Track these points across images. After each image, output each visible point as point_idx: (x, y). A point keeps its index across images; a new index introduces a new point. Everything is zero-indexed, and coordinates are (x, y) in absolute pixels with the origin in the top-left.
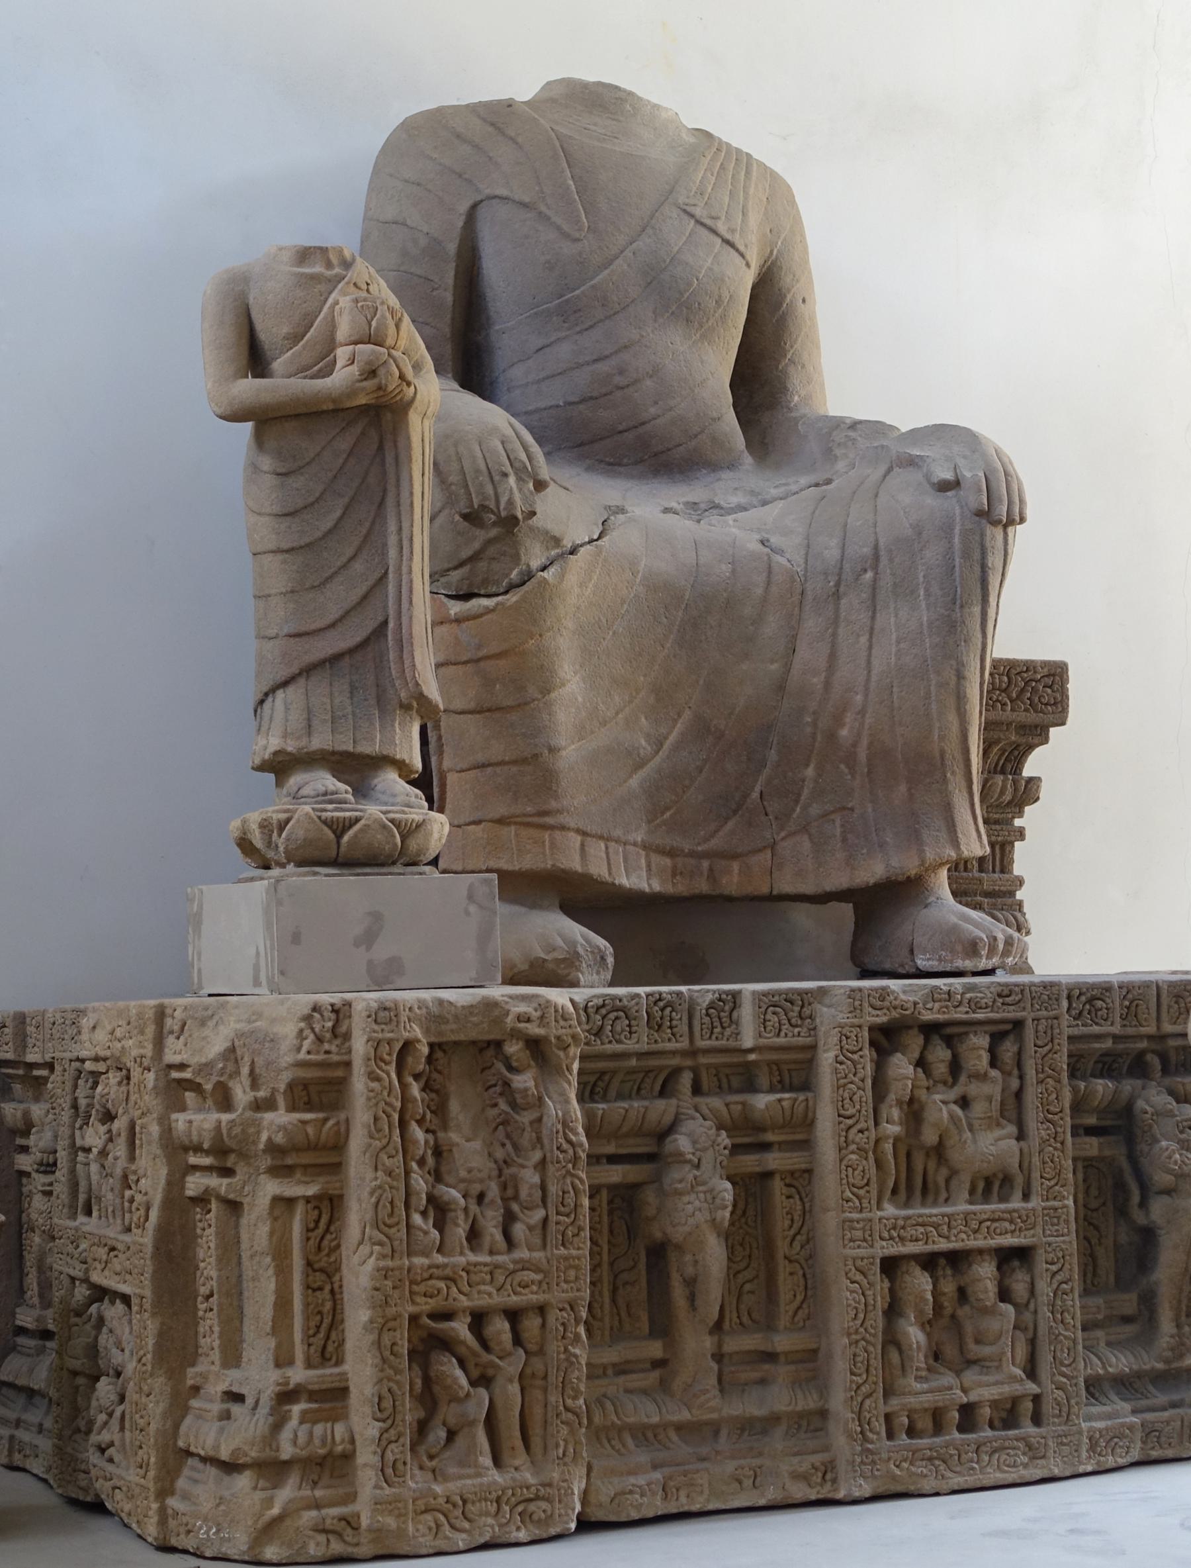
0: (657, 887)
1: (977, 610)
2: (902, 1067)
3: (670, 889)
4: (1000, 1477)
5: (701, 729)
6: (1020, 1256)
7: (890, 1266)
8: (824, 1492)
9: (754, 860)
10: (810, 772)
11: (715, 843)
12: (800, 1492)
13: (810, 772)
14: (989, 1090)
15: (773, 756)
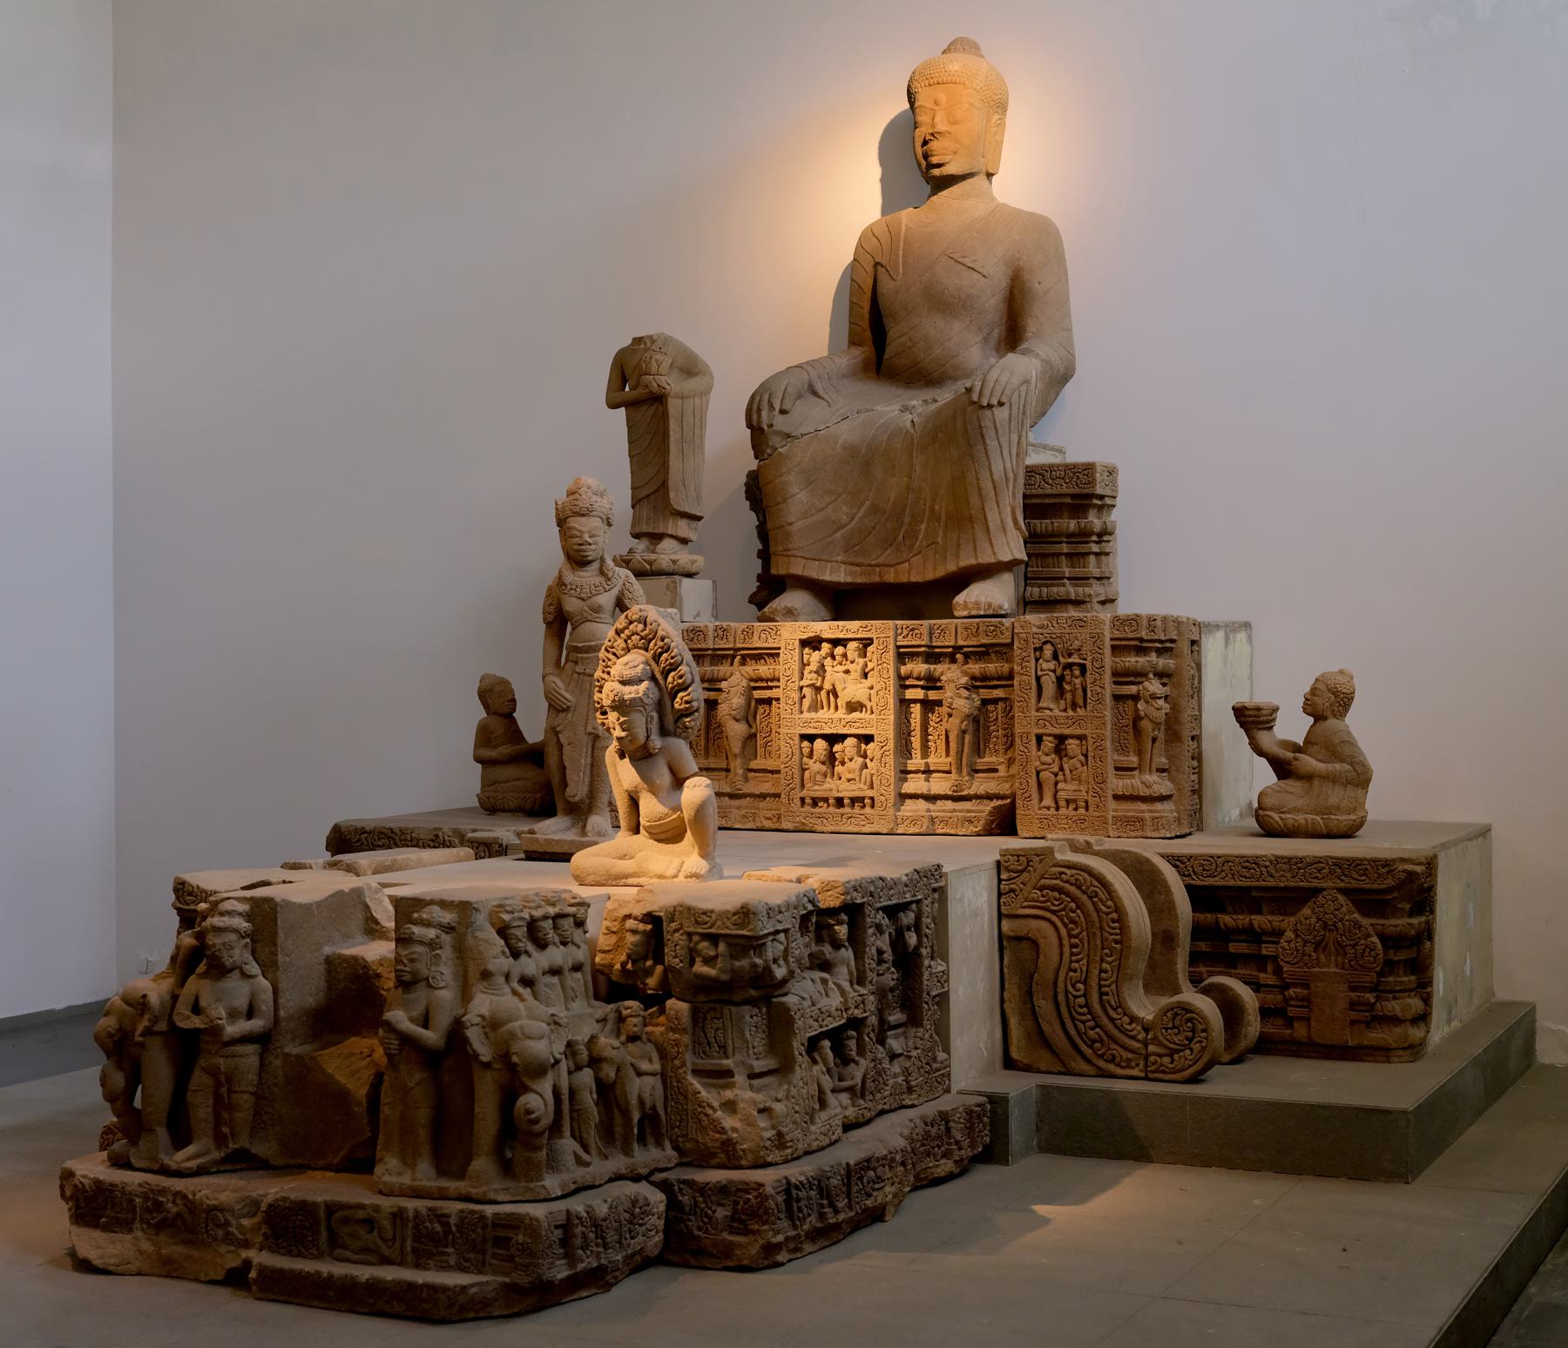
0: (849, 579)
1: (980, 447)
2: (815, 657)
3: (859, 580)
4: (850, 829)
5: (874, 510)
6: (868, 739)
7: (811, 738)
8: (777, 826)
9: (899, 567)
10: (923, 526)
11: (881, 560)
12: (768, 824)
13: (923, 526)
14: (856, 668)
15: (907, 519)
